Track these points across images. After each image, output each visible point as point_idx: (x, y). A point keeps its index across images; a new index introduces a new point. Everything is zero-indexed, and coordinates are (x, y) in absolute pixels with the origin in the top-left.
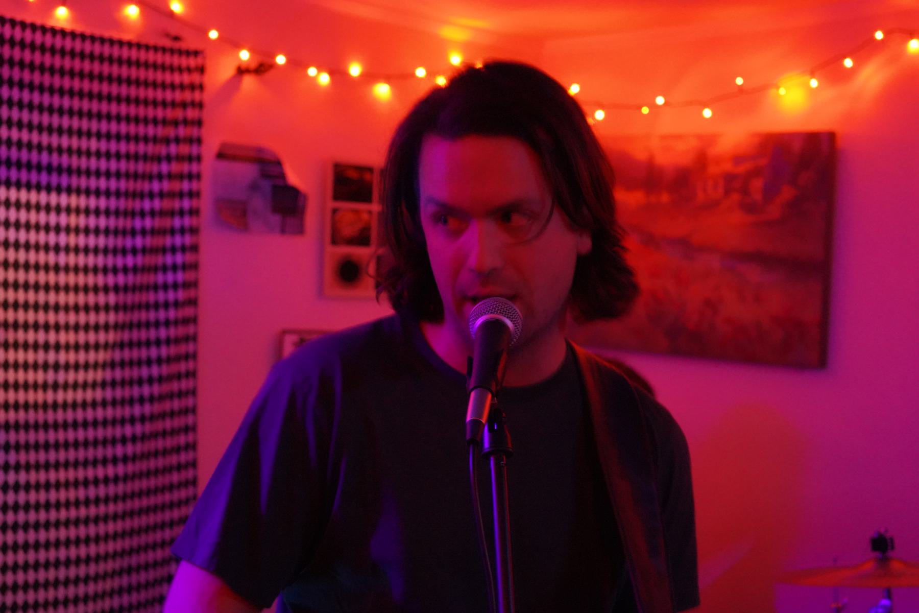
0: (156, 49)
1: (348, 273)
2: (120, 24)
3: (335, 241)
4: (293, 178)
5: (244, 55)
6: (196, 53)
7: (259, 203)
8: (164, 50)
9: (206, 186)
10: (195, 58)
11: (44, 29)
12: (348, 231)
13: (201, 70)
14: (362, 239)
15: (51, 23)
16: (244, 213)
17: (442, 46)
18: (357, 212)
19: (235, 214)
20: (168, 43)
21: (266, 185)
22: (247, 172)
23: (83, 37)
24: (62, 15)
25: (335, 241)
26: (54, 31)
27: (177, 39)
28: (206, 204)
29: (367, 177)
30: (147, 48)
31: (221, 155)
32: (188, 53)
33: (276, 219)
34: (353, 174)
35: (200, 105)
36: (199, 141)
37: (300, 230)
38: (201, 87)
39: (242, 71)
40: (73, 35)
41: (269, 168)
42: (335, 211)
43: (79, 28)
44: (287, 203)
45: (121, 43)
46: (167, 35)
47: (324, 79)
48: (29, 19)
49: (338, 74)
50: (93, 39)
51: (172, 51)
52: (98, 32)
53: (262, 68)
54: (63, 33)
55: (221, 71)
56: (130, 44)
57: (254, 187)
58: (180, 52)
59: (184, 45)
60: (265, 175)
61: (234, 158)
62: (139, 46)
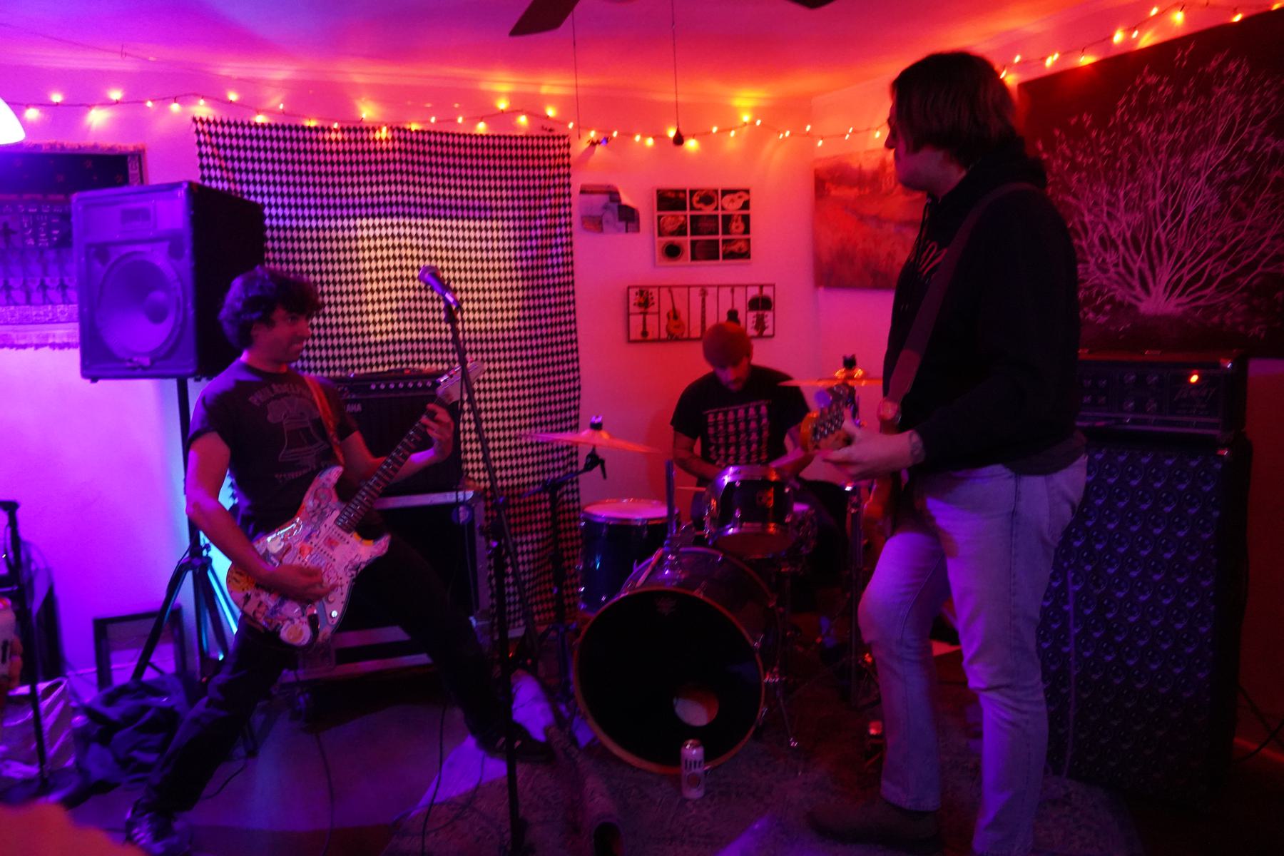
0: (538, 138)
1: (672, 252)
2: (515, 127)
3: (660, 234)
4: (626, 200)
5: (593, 134)
6: (564, 137)
7: (609, 216)
8: (543, 138)
9: (575, 210)
10: (564, 141)
11: (471, 136)
12: (669, 228)
13: (569, 146)
14: (681, 231)
15: (474, 132)
16: (601, 222)
17: (733, 112)
18: (677, 217)
19: (595, 223)
20: (546, 134)
21: (615, 206)
22: (602, 199)
23: (494, 137)
24: (481, 128)
25: (660, 234)
26: (477, 136)
27: (551, 130)
28: (576, 220)
29: (681, 195)
30: (533, 138)
31: (583, 192)
32: (559, 138)
33: (622, 224)
34: (669, 194)
35: (569, 165)
36: (569, 185)
37: (637, 230)
38: (569, 155)
39: (593, 144)
40: (488, 137)
41: (613, 194)
42: (659, 218)
43: (490, 133)
44: (628, 216)
45: (516, 138)
46: (543, 128)
47: (650, 142)
48: (462, 132)
49: (659, 137)
50: (499, 137)
51: (549, 138)
52: (502, 133)
53: (606, 140)
54: (482, 136)
55: (581, 146)
56: (522, 138)
57: (606, 207)
58: (554, 138)
59: (556, 134)
60: (612, 200)
61: (592, 192)
62: (527, 138)
